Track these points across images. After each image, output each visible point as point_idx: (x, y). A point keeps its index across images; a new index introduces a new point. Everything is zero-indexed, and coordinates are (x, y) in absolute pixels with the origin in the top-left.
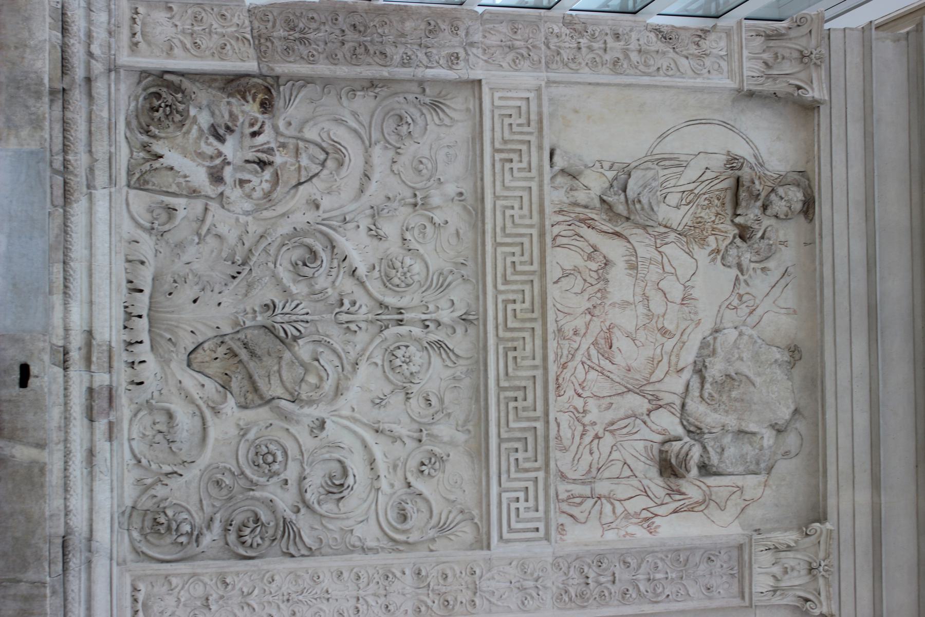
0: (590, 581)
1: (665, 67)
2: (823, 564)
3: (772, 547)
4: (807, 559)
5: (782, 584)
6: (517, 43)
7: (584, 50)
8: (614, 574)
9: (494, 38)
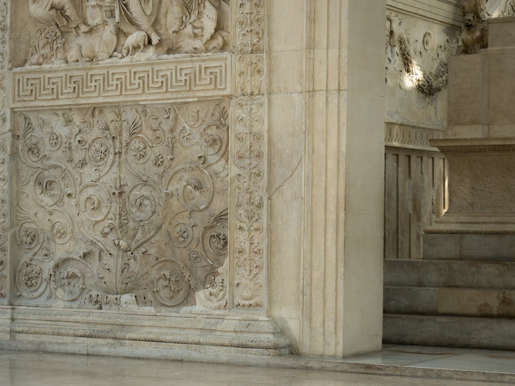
0: (249, 30)
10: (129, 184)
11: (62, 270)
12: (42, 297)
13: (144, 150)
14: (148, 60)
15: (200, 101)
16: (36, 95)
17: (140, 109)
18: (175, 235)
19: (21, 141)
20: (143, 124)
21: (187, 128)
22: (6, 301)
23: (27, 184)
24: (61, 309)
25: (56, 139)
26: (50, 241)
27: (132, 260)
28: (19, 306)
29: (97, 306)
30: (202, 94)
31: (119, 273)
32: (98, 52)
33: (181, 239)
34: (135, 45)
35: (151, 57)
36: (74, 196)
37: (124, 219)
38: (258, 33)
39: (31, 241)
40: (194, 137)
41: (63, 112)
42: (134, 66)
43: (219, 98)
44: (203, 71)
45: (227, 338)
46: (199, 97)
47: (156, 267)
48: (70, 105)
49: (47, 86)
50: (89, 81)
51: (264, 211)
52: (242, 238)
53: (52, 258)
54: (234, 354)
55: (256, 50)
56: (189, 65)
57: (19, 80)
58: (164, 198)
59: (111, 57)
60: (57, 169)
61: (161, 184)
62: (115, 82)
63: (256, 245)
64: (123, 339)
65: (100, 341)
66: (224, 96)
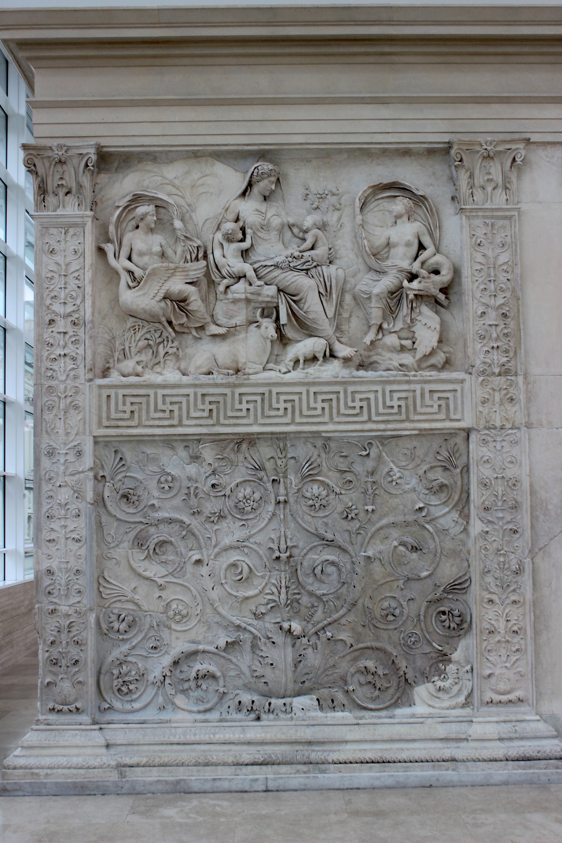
0: (495, 345)
1: (77, 282)
2: (485, 147)
3: (471, 190)
4: (480, 161)
5: (500, 181)
6: (62, 406)
7: (66, 351)
8: (490, 325)
9: (58, 425)
10: (301, 544)
11: (185, 668)
12: (147, 708)
13: (327, 499)
14: (334, 377)
15: (423, 434)
16: (140, 417)
17: (319, 443)
18: (378, 613)
19: (108, 484)
20: (324, 464)
21: (396, 469)
22: (85, 718)
23: (117, 545)
24: (189, 725)
25: (168, 482)
26: (162, 627)
27: (310, 650)
28: (109, 723)
29: (253, 716)
30: (426, 426)
31: (290, 668)
32: (245, 363)
33: (391, 618)
34: (310, 356)
35: (337, 373)
36: (206, 563)
37: (295, 594)
38: (506, 351)
39: (127, 629)
40: (407, 482)
41: (186, 444)
42: (314, 384)
43: (453, 431)
44: (427, 395)
45: (499, 750)
46: (420, 430)
47: (348, 658)
48: (200, 434)
49: (160, 406)
50: (237, 401)
51: (526, 579)
52: (491, 615)
53: (166, 651)
54: (517, 771)
55: (505, 372)
56: (405, 387)
57: (109, 396)
58: (362, 563)
59: (264, 369)
60: (173, 525)
61: (356, 544)
62: (282, 405)
63: (515, 622)
64: (323, 763)
65: (283, 769)
66: (460, 429)
